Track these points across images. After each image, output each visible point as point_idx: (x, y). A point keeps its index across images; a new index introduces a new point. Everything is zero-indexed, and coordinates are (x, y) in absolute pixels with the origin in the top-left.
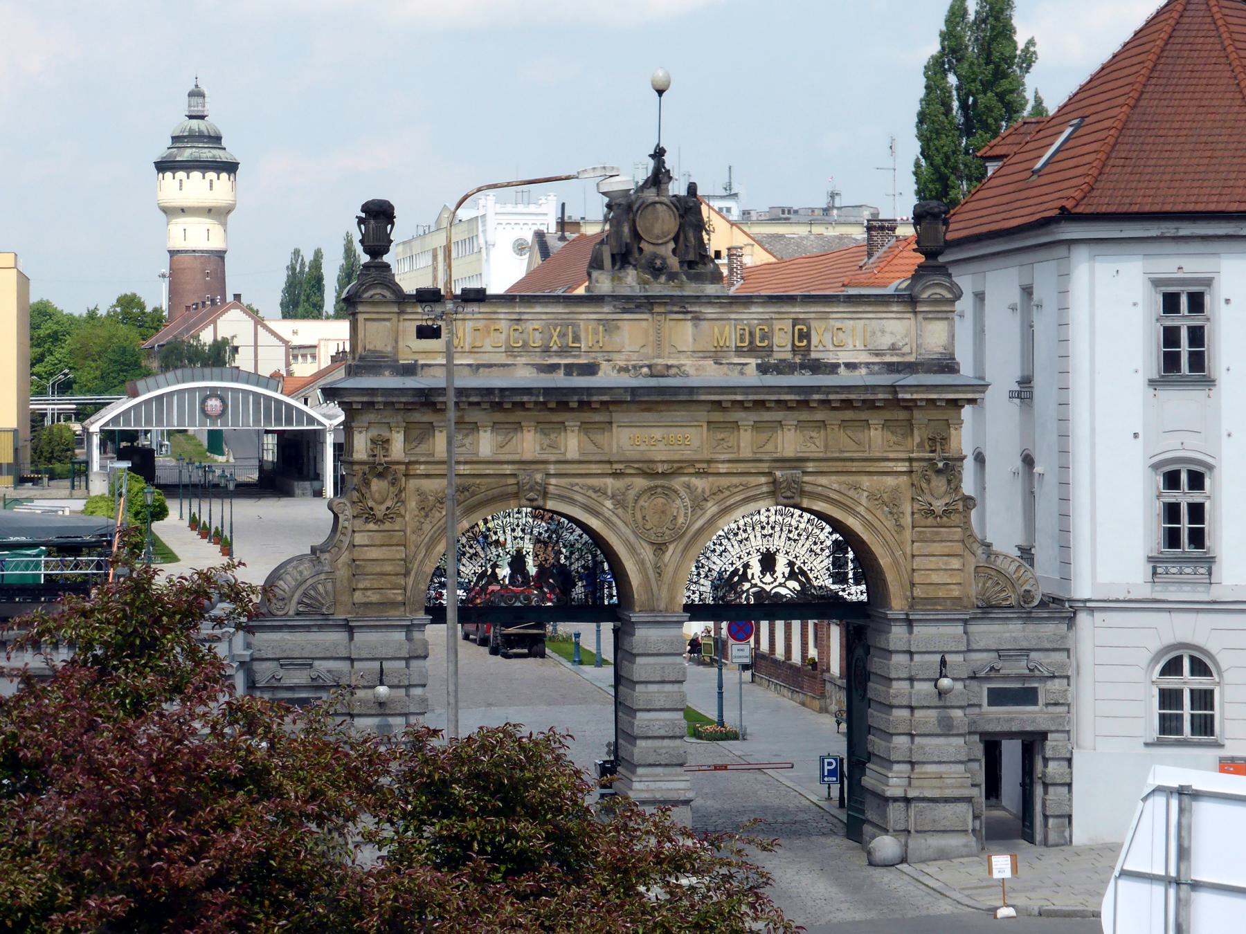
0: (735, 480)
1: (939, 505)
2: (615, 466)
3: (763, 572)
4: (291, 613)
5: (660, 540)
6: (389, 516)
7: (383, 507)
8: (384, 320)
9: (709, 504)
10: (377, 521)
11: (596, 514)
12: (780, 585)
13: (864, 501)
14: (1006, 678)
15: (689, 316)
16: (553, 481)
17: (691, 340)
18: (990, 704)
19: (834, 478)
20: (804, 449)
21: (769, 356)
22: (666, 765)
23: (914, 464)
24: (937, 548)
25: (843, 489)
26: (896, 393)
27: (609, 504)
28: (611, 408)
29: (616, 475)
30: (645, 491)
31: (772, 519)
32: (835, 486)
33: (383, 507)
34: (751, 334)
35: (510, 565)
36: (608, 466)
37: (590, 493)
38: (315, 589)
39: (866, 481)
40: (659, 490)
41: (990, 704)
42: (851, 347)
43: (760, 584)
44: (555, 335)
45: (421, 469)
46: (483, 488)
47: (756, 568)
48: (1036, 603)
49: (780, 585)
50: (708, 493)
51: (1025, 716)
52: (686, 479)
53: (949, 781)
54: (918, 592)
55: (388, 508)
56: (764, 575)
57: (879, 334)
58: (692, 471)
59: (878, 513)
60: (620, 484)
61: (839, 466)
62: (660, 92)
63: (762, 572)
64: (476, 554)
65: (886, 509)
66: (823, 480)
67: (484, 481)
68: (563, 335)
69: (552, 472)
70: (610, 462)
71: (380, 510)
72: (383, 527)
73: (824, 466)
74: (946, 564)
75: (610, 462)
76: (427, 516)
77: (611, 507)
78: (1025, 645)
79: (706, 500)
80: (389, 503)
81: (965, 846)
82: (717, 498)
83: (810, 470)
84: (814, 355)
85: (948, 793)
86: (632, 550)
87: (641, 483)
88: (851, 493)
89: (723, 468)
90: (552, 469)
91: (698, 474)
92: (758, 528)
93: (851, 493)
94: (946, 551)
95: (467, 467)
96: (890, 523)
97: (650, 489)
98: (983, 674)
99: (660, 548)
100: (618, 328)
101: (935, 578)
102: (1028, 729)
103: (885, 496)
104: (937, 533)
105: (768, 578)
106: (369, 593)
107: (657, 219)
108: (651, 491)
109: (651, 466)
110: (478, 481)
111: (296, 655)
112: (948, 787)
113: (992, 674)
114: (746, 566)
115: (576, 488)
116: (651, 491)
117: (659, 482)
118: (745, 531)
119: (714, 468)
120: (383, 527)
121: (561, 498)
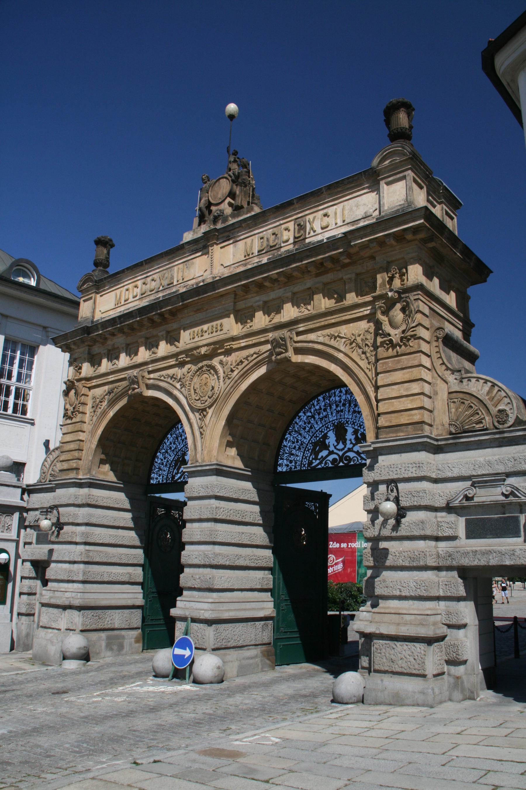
0: (252, 351)
3: (338, 441)
4: (48, 480)
5: (202, 406)
12: (350, 450)
13: (342, 348)
14: (484, 507)
15: (231, 241)
16: (152, 376)
17: (232, 256)
18: (468, 537)
19: (319, 333)
20: (300, 314)
21: (278, 251)
22: (199, 590)
24: (398, 376)
25: (327, 340)
27: (178, 385)
30: (198, 371)
31: (344, 397)
32: (321, 339)
37: (169, 380)
40: (204, 368)
41: (468, 537)
42: (334, 226)
43: (335, 451)
46: (120, 388)
47: (332, 439)
48: (511, 421)
49: (350, 450)
50: (234, 364)
51: (503, 548)
52: (222, 357)
53: (407, 617)
54: (383, 421)
56: (338, 443)
57: (355, 208)
59: (354, 356)
61: (323, 322)
63: (336, 441)
65: (360, 351)
66: (312, 337)
69: (150, 369)
72: (74, 420)
73: (311, 325)
74: (407, 389)
78: (501, 469)
81: (423, 693)
82: (240, 367)
83: (301, 329)
84: (307, 241)
85: (404, 631)
89: (243, 343)
90: (151, 367)
91: (228, 352)
92: (334, 407)
93: (333, 343)
94: (407, 377)
96: (363, 364)
97: (200, 369)
98: (456, 503)
100: (193, 263)
101: (398, 405)
102: (508, 563)
103: (359, 340)
104: (399, 362)
105: (341, 446)
106: (63, 463)
107: (220, 188)
109: (198, 351)
112: (405, 624)
113: (466, 503)
114: (325, 437)
115: (162, 378)
117: (205, 363)
118: (325, 410)
119: (235, 345)
120: (74, 420)
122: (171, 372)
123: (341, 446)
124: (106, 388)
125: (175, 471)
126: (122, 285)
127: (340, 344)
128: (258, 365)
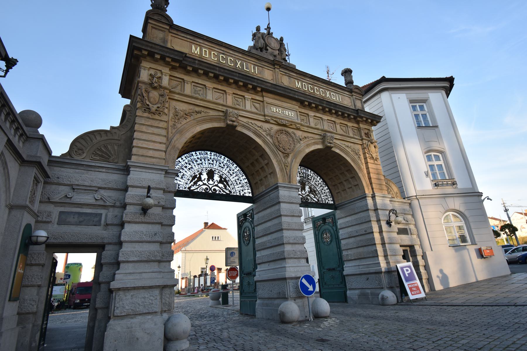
1: (374, 155)
2: (266, 118)
6: (158, 112)
7: (155, 106)
8: (161, 30)
9: (302, 142)
10: (150, 112)
11: (259, 136)
23: (364, 141)
25: (344, 146)
26: (358, 113)
28: (264, 94)
29: (267, 122)
33: (155, 106)
34: (308, 87)
35: (207, 174)
36: (264, 118)
38: (106, 147)
39: (350, 144)
44: (239, 64)
45: (177, 97)
52: (292, 130)
55: (158, 107)
58: (295, 128)
60: (266, 126)
62: (268, 9)
64: (192, 168)
67: (208, 111)
68: (242, 65)
70: (265, 116)
71: (154, 108)
75: (265, 116)
76: (179, 119)
77: (265, 135)
79: (301, 140)
80: (159, 105)
86: (275, 155)
87: (276, 128)
88: (347, 148)
89: (306, 129)
93: (347, 148)
95: (202, 102)
99: (287, 155)
105: (303, 192)
108: (281, 131)
110: (205, 110)
111: (87, 184)
115: (250, 124)
116: (281, 131)
119: (302, 128)
121: (244, 126)
122: (259, 124)
123: (303, 192)
124: (192, 107)
125: (192, 183)
126: (198, 43)
127: (349, 150)
128: (315, 143)
